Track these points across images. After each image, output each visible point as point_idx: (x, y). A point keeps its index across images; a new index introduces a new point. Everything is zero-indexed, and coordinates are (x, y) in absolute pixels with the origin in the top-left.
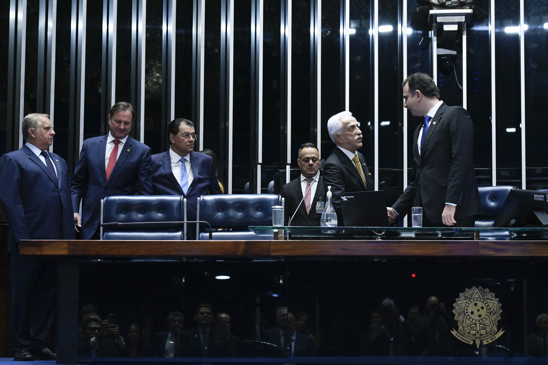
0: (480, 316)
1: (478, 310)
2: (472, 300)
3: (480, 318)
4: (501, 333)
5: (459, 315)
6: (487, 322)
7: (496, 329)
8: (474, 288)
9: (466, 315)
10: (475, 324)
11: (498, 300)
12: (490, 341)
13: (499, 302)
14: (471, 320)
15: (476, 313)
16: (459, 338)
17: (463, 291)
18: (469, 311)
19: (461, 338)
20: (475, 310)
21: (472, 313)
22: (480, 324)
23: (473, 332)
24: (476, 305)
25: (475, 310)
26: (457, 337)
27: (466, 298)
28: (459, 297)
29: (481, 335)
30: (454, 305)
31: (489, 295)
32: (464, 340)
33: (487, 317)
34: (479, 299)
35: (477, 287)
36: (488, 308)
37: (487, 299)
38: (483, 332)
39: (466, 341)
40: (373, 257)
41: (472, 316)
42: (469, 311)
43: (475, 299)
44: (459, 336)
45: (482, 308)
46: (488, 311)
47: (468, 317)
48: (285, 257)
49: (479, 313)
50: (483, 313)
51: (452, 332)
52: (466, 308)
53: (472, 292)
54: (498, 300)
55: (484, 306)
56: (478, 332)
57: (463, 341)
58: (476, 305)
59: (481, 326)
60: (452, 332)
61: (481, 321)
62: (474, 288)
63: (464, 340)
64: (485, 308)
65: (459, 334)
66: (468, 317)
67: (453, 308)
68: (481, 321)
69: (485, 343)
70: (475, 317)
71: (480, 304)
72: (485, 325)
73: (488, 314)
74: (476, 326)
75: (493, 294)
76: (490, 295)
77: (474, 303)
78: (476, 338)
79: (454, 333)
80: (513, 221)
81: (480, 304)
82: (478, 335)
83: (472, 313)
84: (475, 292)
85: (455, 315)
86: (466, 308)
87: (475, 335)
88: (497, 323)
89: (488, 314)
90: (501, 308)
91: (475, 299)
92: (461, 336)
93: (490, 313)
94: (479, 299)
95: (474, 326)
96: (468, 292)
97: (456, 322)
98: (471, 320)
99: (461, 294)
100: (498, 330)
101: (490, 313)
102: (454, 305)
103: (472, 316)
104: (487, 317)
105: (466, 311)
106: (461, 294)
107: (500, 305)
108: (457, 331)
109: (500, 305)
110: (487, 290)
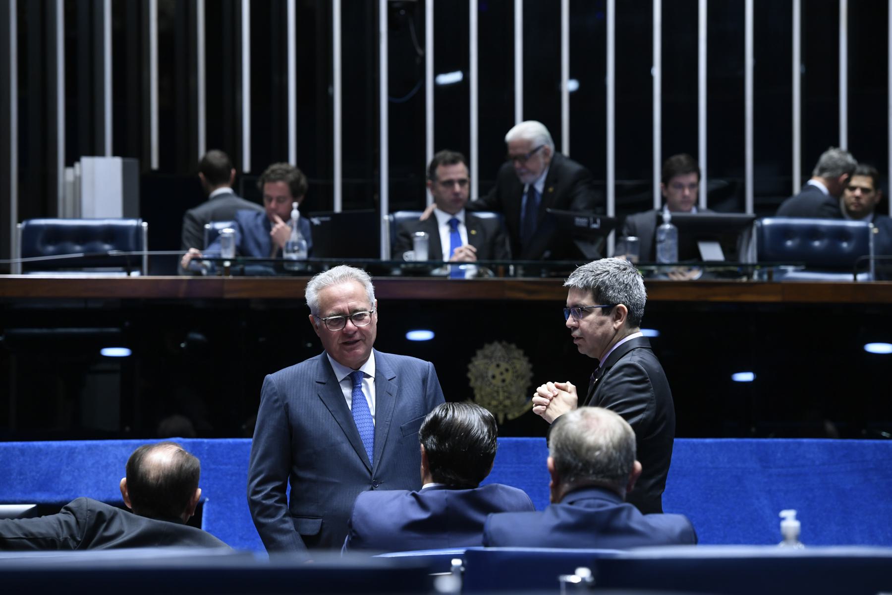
0: (504, 381)
1: (502, 374)
5: (476, 379)
6: (513, 389)
10: (498, 392)
13: (530, 361)
18: (490, 374)
20: (497, 372)
21: (494, 377)
22: (504, 392)
23: (494, 403)
24: (498, 366)
25: (497, 372)
27: (486, 357)
28: (475, 355)
30: (470, 366)
35: (500, 342)
37: (514, 358)
38: (507, 402)
40: (247, 301)
42: (490, 374)
45: (507, 370)
48: (267, 301)
50: (508, 377)
58: (498, 366)
69: (510, 417)
70: (497, 382)
71: (504, 365)
76: (518, 353)
80: (547, 254)
81: (504, 365)
82: (501, 407)
83: (494, 377)
84: (496, 349)
90: (532, 370)
96: (489, 349)
102: (470, 366)
103: (494, 382)
110: (513, 346)
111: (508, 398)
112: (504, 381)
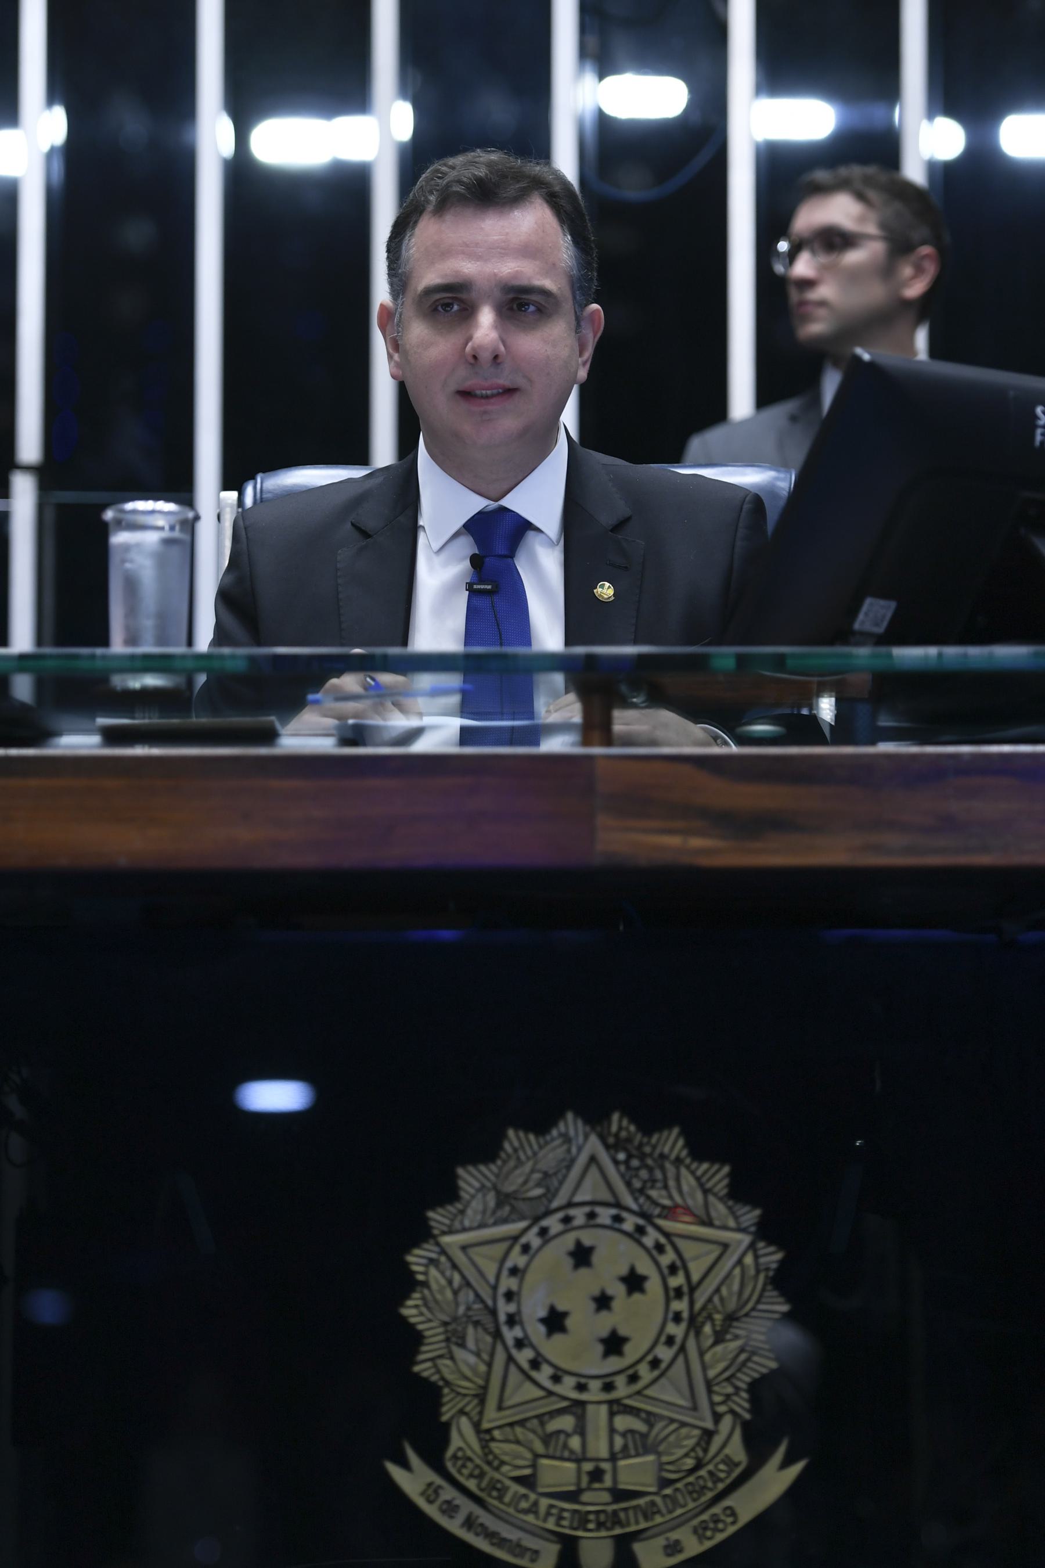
0: (614, 1344)
1: (603, 1302)
2: (553, 1223)
3: (614, 1363)
4: (775, 1481)
6: (669, 1394)
7: (737, 1450)
8: (571, 1124)
9: (510, 1335)
10: (577, 1408)
11: (751, 1216)
12: (693, 1547)
13: (765, 1232)
14: (543, 1375)
15: (586, 1325)
16: (454, 1526)
17: (487, 1151)
18: (534, 1308)
19: (469, 1523)
21: (555, 1321)
22: (616, 1407)
23: (559, 1473)
24: (582, 1256)
26: (432, 1511)
27: (507, 1203)
28: (449, 1194)
29: (620, 1495)
30: (416, 1259)
31: (688, 1181)
32: (491, 1536)
33: (665, 1353)
34: (605, 1215)
36: (677, 1281)
37: (669, 1212)
38: (636, 1472)
39: (501, 1542)
41: (555, 1348)
43: (579, 1215)
44: (449, 1509)
46: (681, 1306)
47: (524, 1357)
49: (604, 1323)
50: (641, 1318)
51: (395, 1471)
52: (508, 1283)
53: (551, 1153)
54: (751, 1216)
55: (645, 1267)
56: (596, 1475)
57: (482, 1544)
58: (582, 1256)
59: (622, 1422)
60: (395, 1471)
61: (622, 1389)
62: (571, 1124)
63: (491, 1536)
64: (654, 1285)
65: (449, 1493)
66: (524, 1357)
67: (408, 1283)
68: (622, 1389)
70: (577, 1351)
71: (615, 1255)
72: (650, 1419)
73: (677, 1331)
74: (581, 1430)
75: (720, 1176)
77: (569, 1241)
78: (582, 1521)
79: (412, 1480)
81: (615, 1255)
82: (596, 1499)
83: (555, 1321)
84: (575, 1159)
85: (414, 1338)
86: (508, 1283)
87: (572, 1496)
88: (742, 1404)
89: (677, 1331)
91: (579, 1215)
92: (467, 1506)
93: (694, 1324)
94: (605, 1215)
95: (566, 1422)
97: (430, 1394)
98: (543, 1375)
99: (470, 1179)
100: (757, 1459)
101: (694, 1324)
103: (555, 1348)
104: (665, 1353)
105: (504, 1309)
106: (470, 1179)
107: (772, 1257)
108: (435, 1459)
109: (772, 1257)
110: (672, 1142)
111: (642, 1444)
112: (614, 1344)
